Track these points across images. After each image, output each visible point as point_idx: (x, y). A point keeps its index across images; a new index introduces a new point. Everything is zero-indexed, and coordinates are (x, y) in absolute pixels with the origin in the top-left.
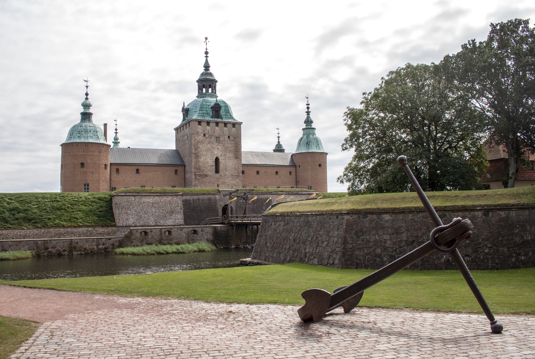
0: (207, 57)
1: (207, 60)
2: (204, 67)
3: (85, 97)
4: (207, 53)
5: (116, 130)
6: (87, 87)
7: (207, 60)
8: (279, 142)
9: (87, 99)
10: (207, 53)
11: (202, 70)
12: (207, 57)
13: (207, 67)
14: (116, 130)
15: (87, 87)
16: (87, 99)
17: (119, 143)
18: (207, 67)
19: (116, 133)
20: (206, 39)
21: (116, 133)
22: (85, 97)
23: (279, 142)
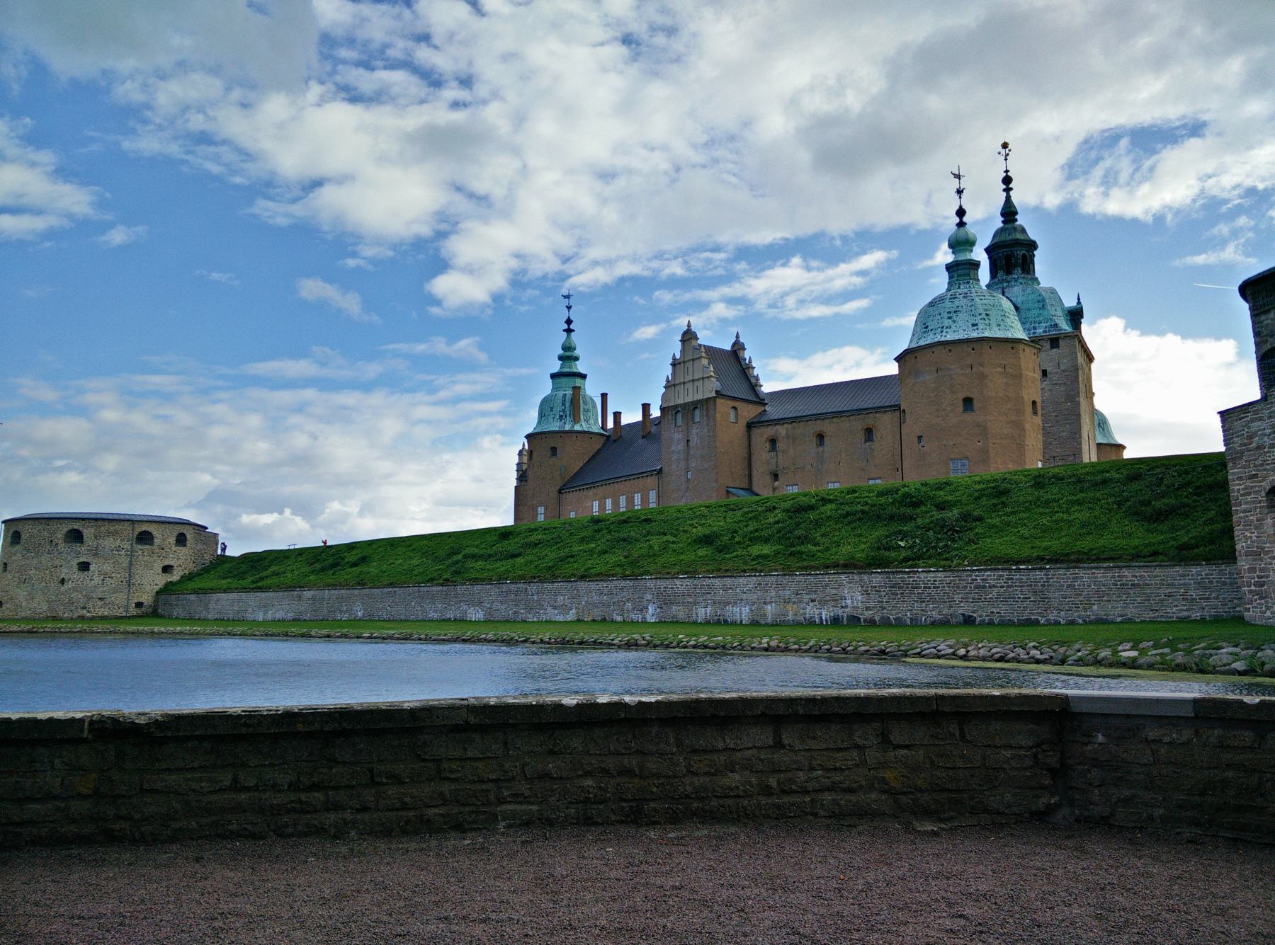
0: (1008, 190)
1: (1008, 199)
2: (1003, 215)
3: (957, 220)
4: (1007, 180)
5: (569, 322)
6: (960, 192)
7: (1008, 199)
9: (961, 224)
10: (1007, 180)
12: (1008, 190)
14: (569, 322)
15: (960, 192)
16: (961, 224)
17: (577, 359)
18: (1009, 213)
20: (1005, 146)
21: (569, 331)
22: (957, 220)
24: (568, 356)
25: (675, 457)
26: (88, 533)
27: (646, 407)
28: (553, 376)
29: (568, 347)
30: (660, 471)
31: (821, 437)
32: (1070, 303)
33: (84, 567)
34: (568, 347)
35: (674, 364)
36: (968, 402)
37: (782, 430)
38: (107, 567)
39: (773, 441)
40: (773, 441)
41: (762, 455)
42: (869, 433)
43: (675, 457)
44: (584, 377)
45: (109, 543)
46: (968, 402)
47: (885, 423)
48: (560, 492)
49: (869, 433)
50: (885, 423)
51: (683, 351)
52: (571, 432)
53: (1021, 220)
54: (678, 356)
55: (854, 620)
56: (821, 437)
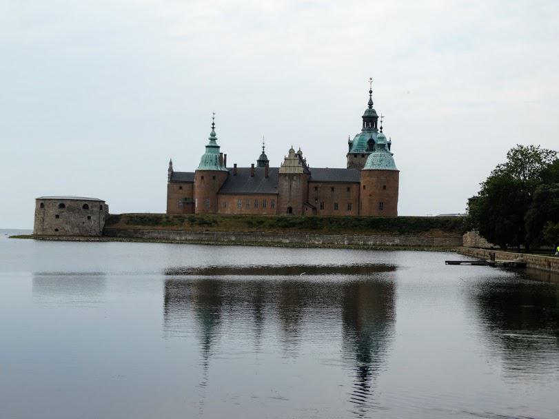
1: (371, 99)
4: (371, 92)
5: (213, 124)
7: (371, 99)
8: (263, 152)
10: (371, 92)
11: (367, 107)
13: (371, 104)
14: (213, 124)
17: (216, 139)
18: (371, 104)
19: (213, 128)
20: (371, 79)
21: (213, 128)
23: (263, 152)
24: (213, 139)
25: (285, 190)
26: (90, 205)
27: (253, 165)
28: (207, 147)
29: (213, 135)
30: (278, 195)
31: (333, 189)
32: (388, 140)
33: (89, 218)
34: (213, 135)
35: (285, 159)
36: (385, 187)
37: (320, 185)
38: (95, 219)
39: (316, 188)
40: (316, 188)
41: (312, 192)
42: (349, 189)
43: (285, 190)
44: (219, 147)
45: (95, 209)
46: (385, 187)
47: (354, 187)
48: (218, 193)
49: (349, 189)
50: (354, 187)
51: (290, 156)
52: (221, 171)
53: (374, 107)
54: (287, 156)
55: (397, 245)
56: (333, 189)
